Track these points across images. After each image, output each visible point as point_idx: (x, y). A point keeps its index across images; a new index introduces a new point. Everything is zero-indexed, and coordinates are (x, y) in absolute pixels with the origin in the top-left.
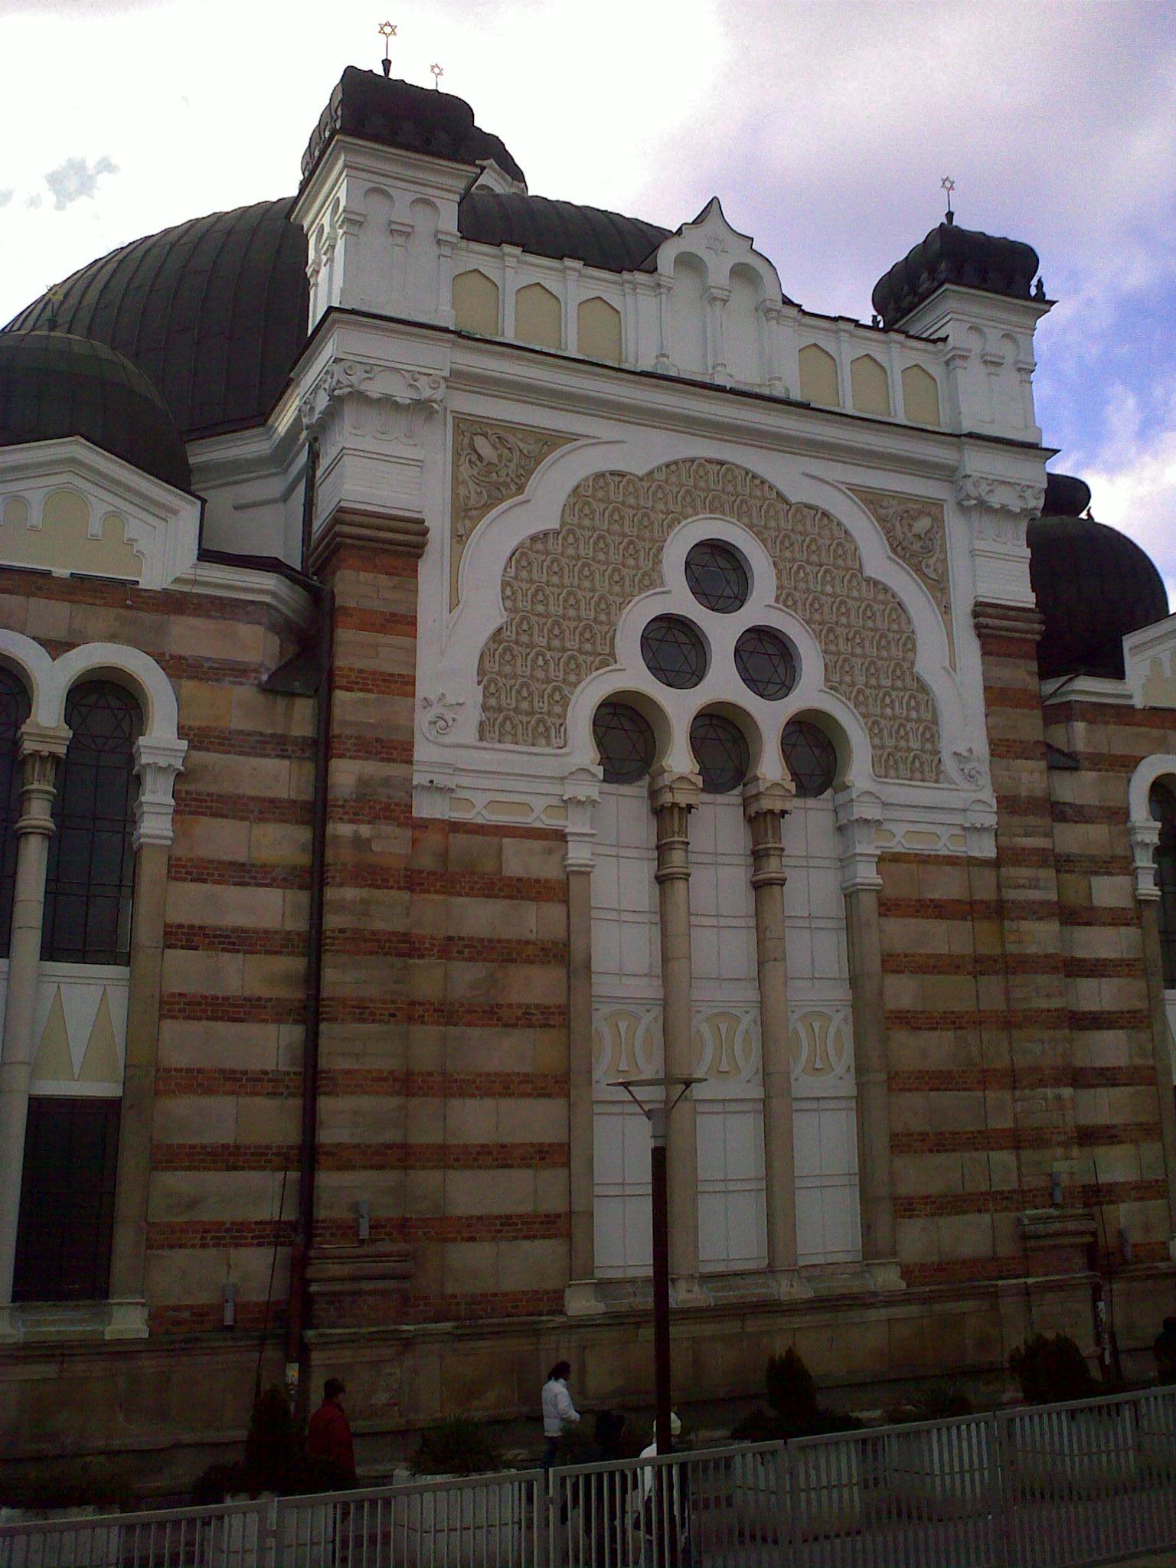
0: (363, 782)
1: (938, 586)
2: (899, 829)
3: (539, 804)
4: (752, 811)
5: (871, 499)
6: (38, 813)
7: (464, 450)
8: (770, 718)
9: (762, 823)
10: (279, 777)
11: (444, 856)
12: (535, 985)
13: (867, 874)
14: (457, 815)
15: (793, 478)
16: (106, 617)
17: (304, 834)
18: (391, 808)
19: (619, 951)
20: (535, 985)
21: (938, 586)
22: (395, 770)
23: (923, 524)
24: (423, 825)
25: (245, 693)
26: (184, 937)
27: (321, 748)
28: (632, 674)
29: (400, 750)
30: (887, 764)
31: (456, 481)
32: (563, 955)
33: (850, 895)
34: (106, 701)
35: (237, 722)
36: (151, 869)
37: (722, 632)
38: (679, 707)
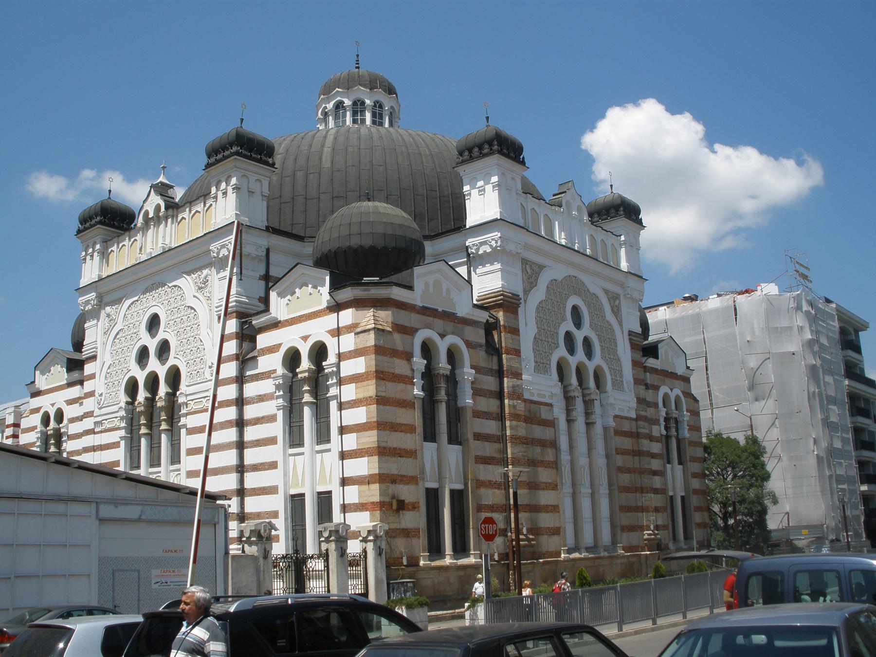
0: (513, 387)
1: (621, 324)
2: (617, 407)
3: (547, 394)
4: (587, 398)
5: (607, 292)
6: (442, 395)
7: (524, 270)
8: (591, 366)
9: (588, 404)
10: (490, 383)
11: (530, 411)
12: (550, 455)
13: (611, 419)
14: (531, 398)
15: (594, 285)
16: (450, 326)
17: (497, 402)
18: (516, 394)
19: (563, 443)
20: (550, 455)
21: (621, 324)
22: (519, 382)
23: (617, 302)
24: (525, 401)
25: (482, 353)
26: (478, 437)
27: (500, 374)
28: (561, 351)
29: (518, 375)
30: (613, 383)
31: (523, 282)
32: (554, 444)
33: (606, 429)
34: (452, 356)
35: (482, 364)
36: (469, 414)
37: (579, 336)
38: (573, 361)
